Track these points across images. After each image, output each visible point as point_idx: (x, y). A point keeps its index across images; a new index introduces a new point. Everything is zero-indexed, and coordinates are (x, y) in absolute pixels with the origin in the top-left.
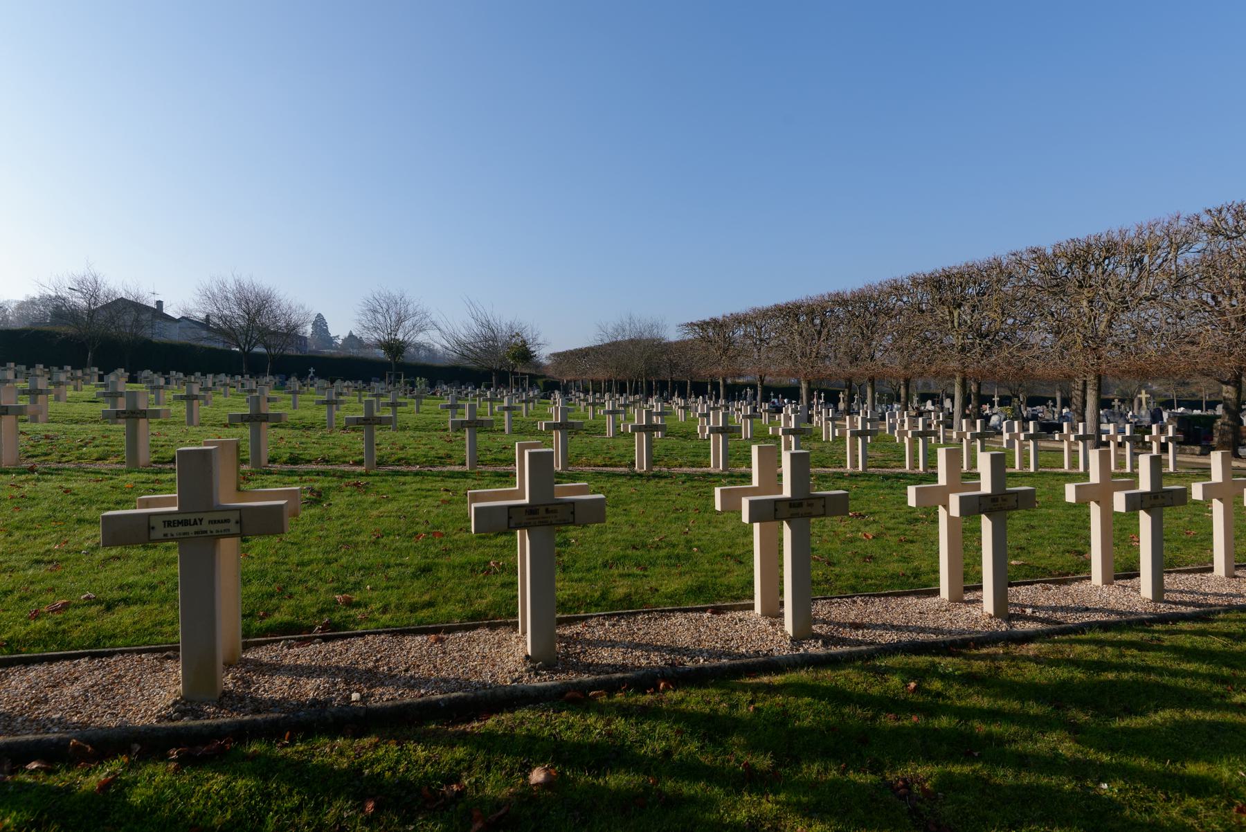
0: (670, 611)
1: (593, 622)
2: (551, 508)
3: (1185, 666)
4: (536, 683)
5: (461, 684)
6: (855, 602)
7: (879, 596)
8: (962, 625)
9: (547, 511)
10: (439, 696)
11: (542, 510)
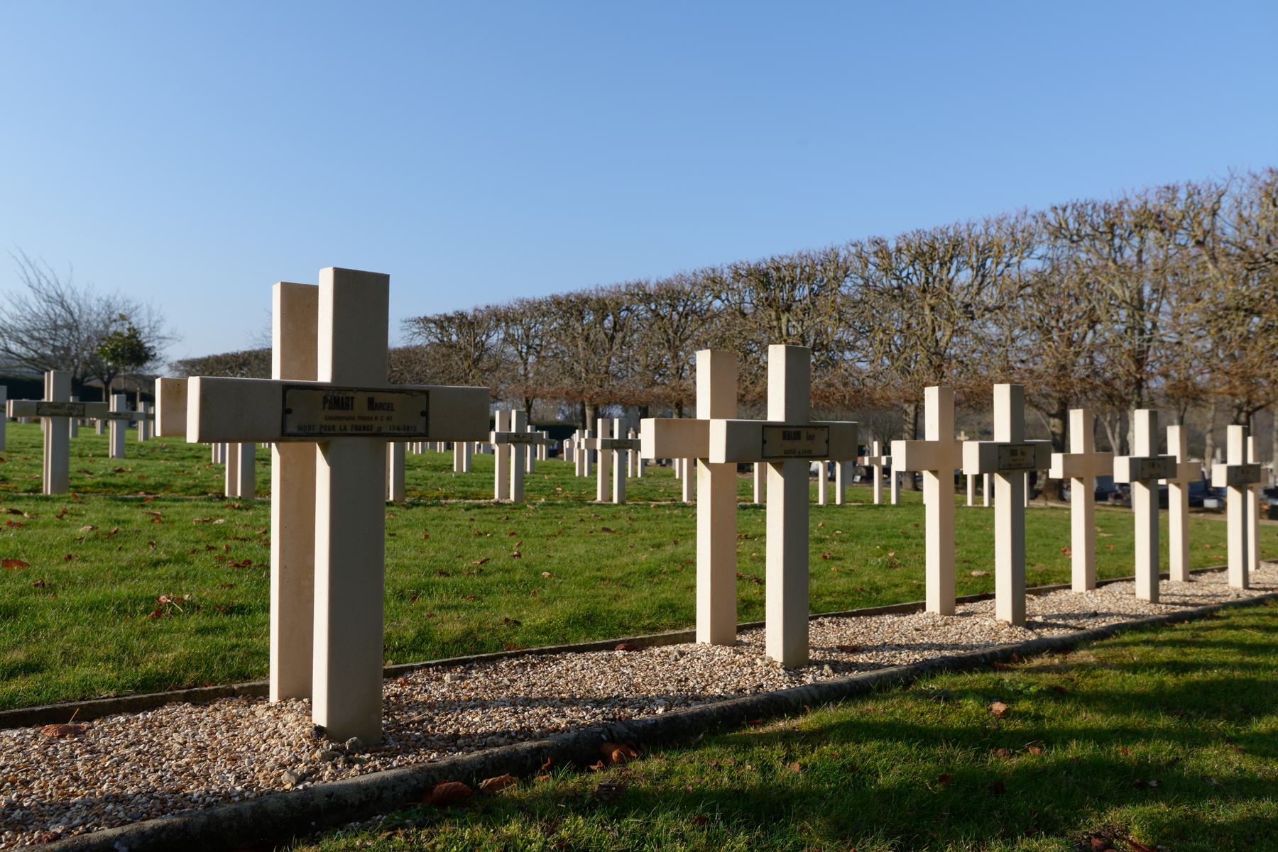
0: (555, 651)
1: (419, 677)
2: (379, 398)
3: (1254, 659)
4: (353, 777)
5: (159, 803)
6: (822, 624)
7: (850, 615)
8: (978, 639)
9: (371, 404)
10: (109, 832)
11: (360, 401)
